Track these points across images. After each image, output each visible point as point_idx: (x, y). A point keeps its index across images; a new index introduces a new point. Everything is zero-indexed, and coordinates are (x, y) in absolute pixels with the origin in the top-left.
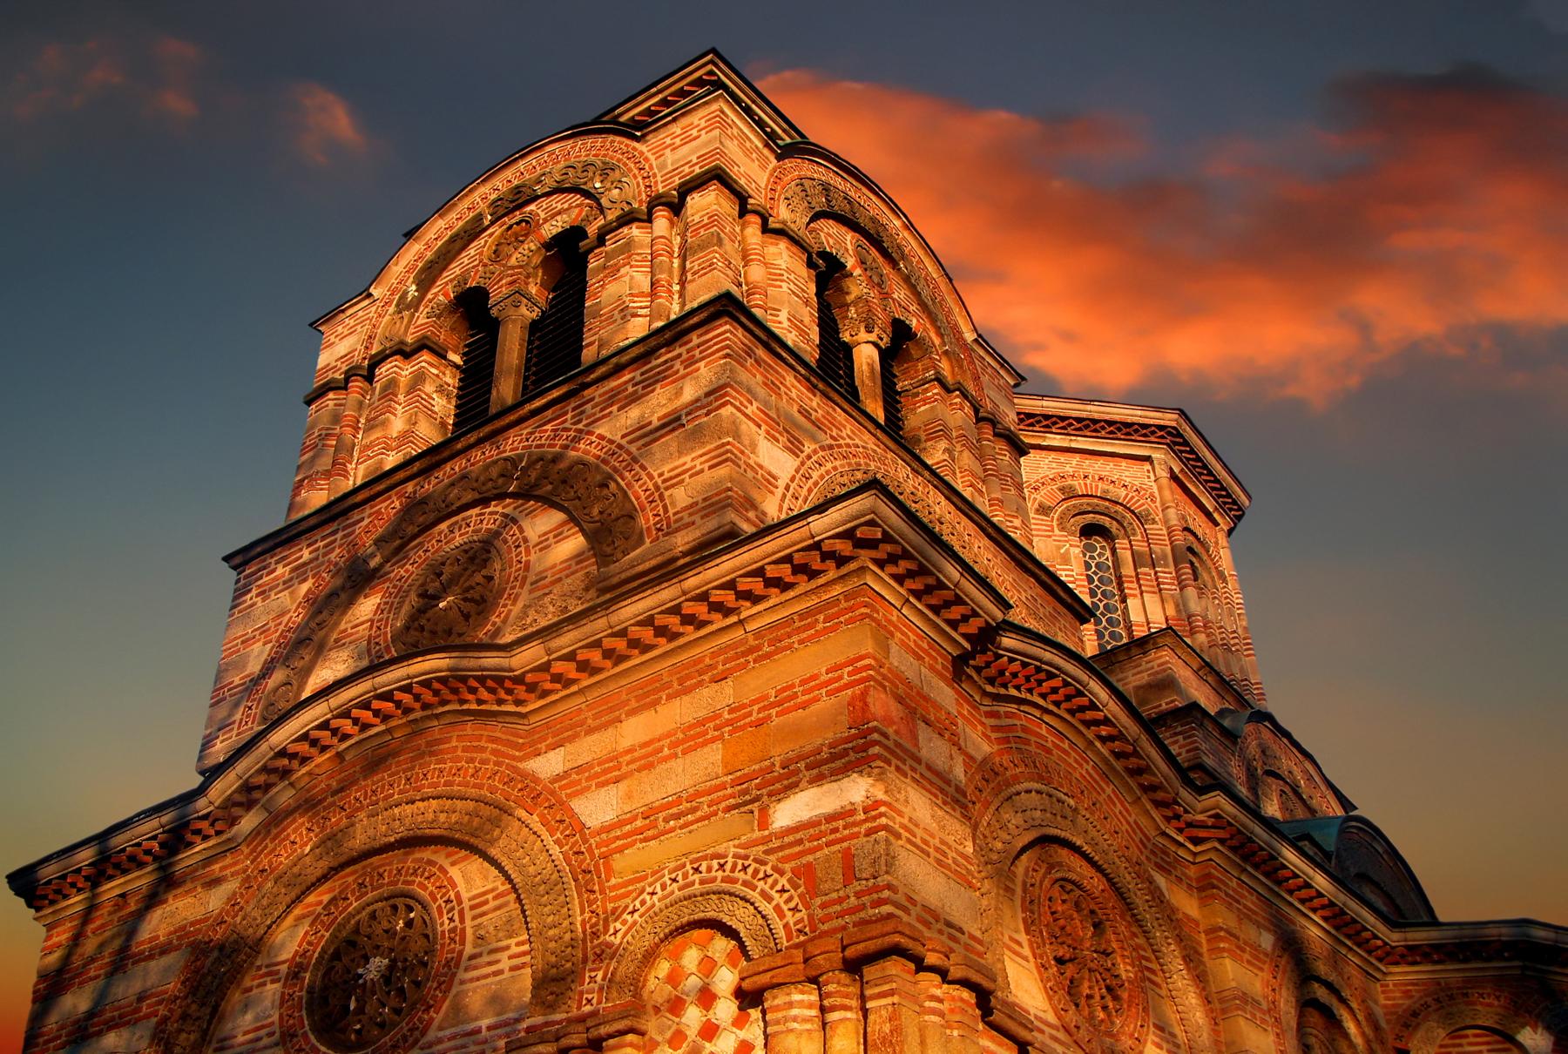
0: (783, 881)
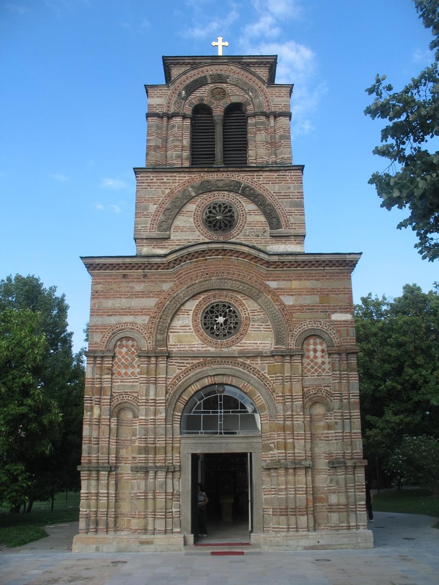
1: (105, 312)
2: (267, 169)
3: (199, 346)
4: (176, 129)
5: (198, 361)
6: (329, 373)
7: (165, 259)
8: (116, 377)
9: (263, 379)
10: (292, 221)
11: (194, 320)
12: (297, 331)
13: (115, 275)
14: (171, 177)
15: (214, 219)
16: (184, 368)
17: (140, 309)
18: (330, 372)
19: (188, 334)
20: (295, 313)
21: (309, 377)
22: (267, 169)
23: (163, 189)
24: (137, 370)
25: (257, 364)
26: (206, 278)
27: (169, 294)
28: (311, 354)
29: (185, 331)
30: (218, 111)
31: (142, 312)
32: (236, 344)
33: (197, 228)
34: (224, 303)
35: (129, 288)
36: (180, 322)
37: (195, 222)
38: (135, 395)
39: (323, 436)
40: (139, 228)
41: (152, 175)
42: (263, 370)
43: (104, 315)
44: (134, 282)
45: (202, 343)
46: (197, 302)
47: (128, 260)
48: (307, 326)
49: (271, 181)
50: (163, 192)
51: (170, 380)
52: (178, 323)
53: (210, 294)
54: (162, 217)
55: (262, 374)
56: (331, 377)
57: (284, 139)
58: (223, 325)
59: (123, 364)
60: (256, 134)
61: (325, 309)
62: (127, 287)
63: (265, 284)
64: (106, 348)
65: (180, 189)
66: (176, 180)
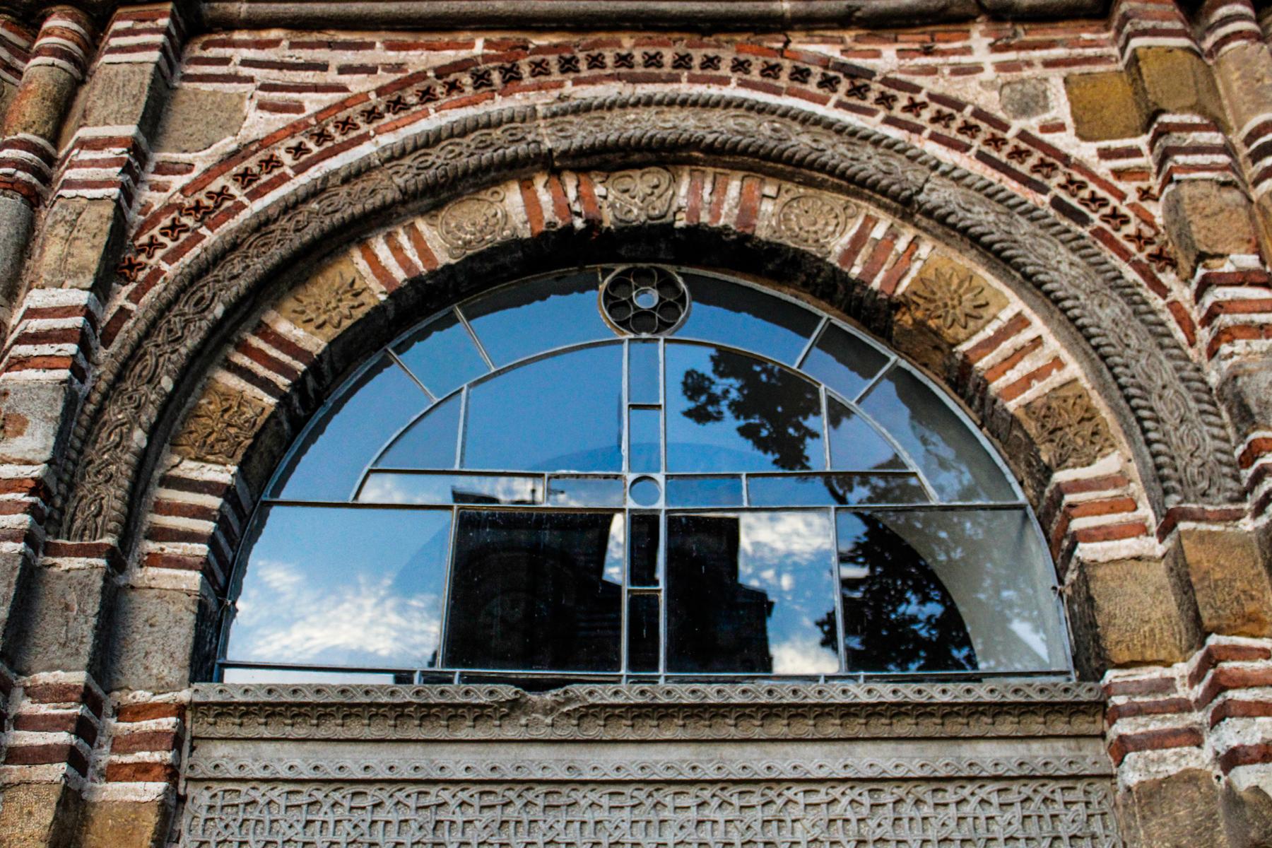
42: (1024, 110)
55: (1023, 135)
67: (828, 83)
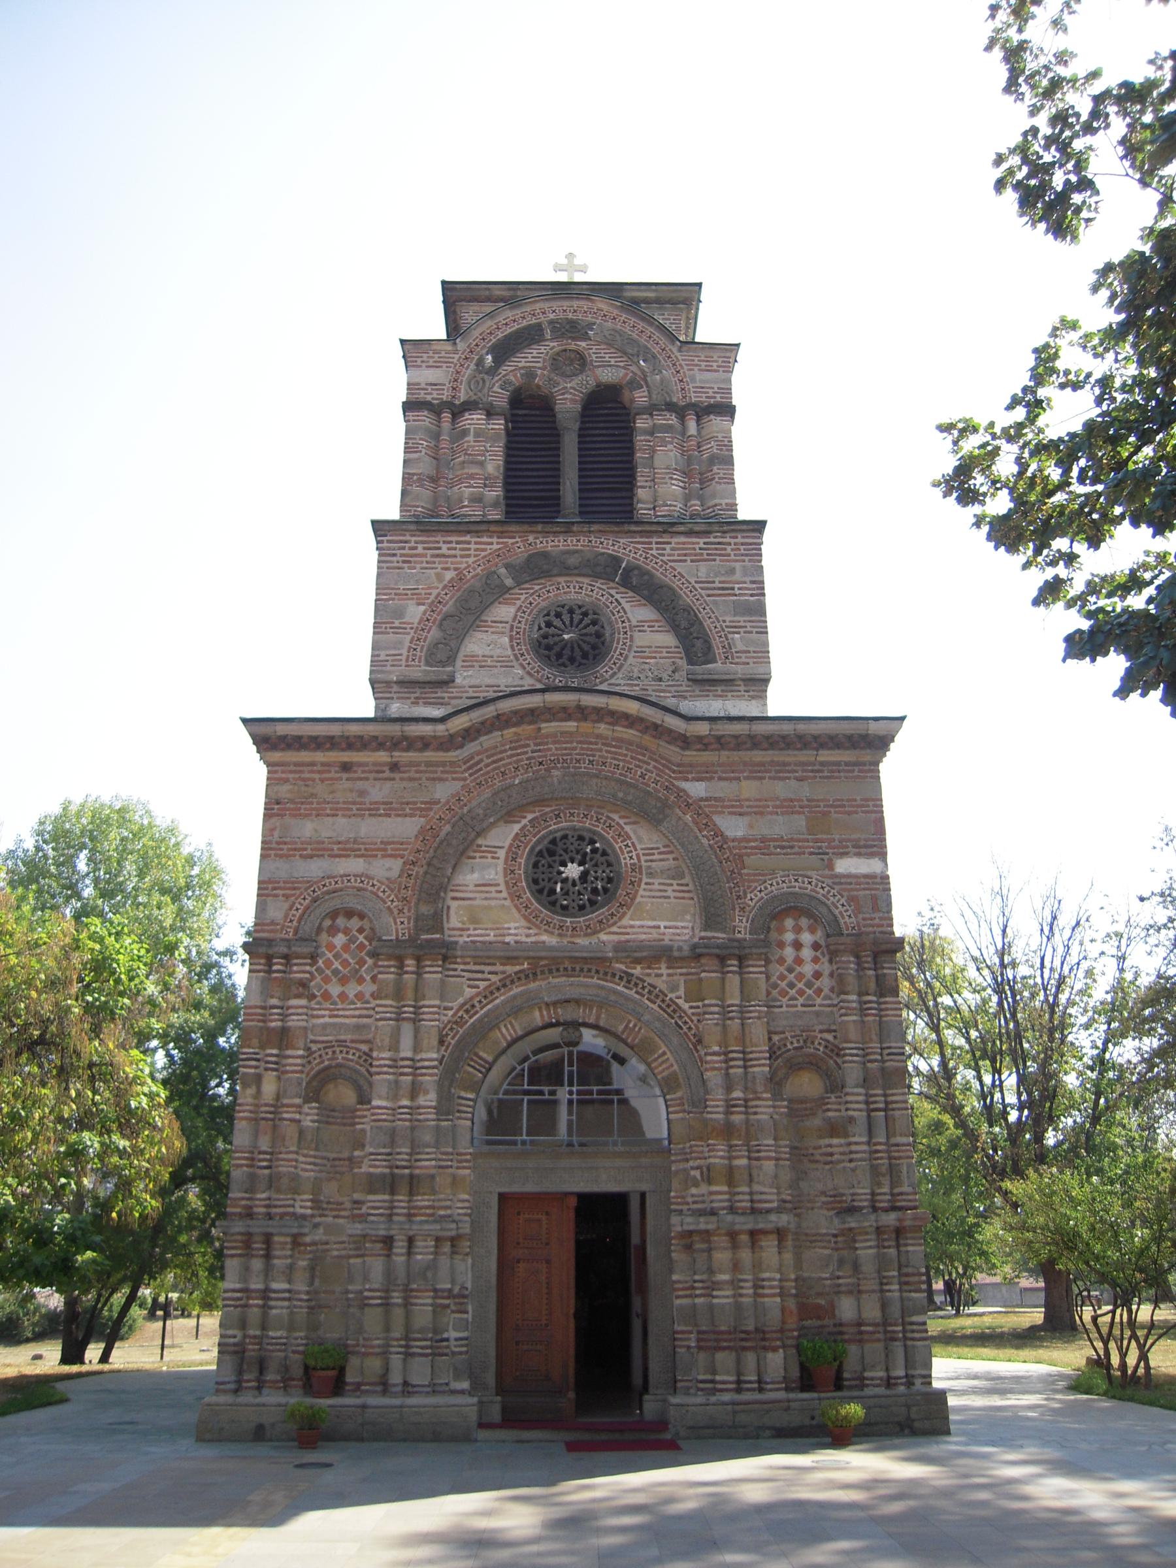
0: (843, 901)
1: (295, 849)
2: (682, 528)
3: (520, 931)
4: (470, 438)
5: (518, 968)
6: (830, 999)
7: (440, 728)
8: (318, 1003)
9: (674, 1011)
10: (740, 646)
11: (509, 871)
12: (754, 899)
13: (323, 764)
14: (458, 543)
15: (557, 639)
16: (482, 984)
17: (382, 842)
18: (834, 996)
19: (493, 903)
20: (748, 855)
21: (784, 1009)
22: (682, 528)
23: (439, 570)
24: (369, 988)
25: (657, 975)
26: (537, 771)
27: (450, 809)
28: (789, 952)
29: (488, 895)
30: (568, 398)
31: (385, 850)
32: (609, 926)
33: (517, 659)
34: (580, 833)
35: (354, 794)
36: (476, 875)
37: (512, 647)
38: (364, 1048)
39: (820, 1151)
40: (382, 658)
41: (413, 539)
42: (672, 991)
43: (294, 856)
44: (367, 779)
45: (524, 923)
46: (516, 828)
47: (354, 729)
48: (778, 886)
49: (690, 555)
50: (439, 577)
51: (451, 1013)
52: (469, 878)
53: (548, 809)
54: (434, 634)
55: (671, 999)
56: (835, 1009)
57: (720, 463)
58: (578, 882)
59: (336, 972)
60: (654, 451)
61: (820, 848)
62: (351, 791)
63: (678, 788)
64: (296, 933)
65: (479, 570)
66: (469, 549)
67: (621, 978)
